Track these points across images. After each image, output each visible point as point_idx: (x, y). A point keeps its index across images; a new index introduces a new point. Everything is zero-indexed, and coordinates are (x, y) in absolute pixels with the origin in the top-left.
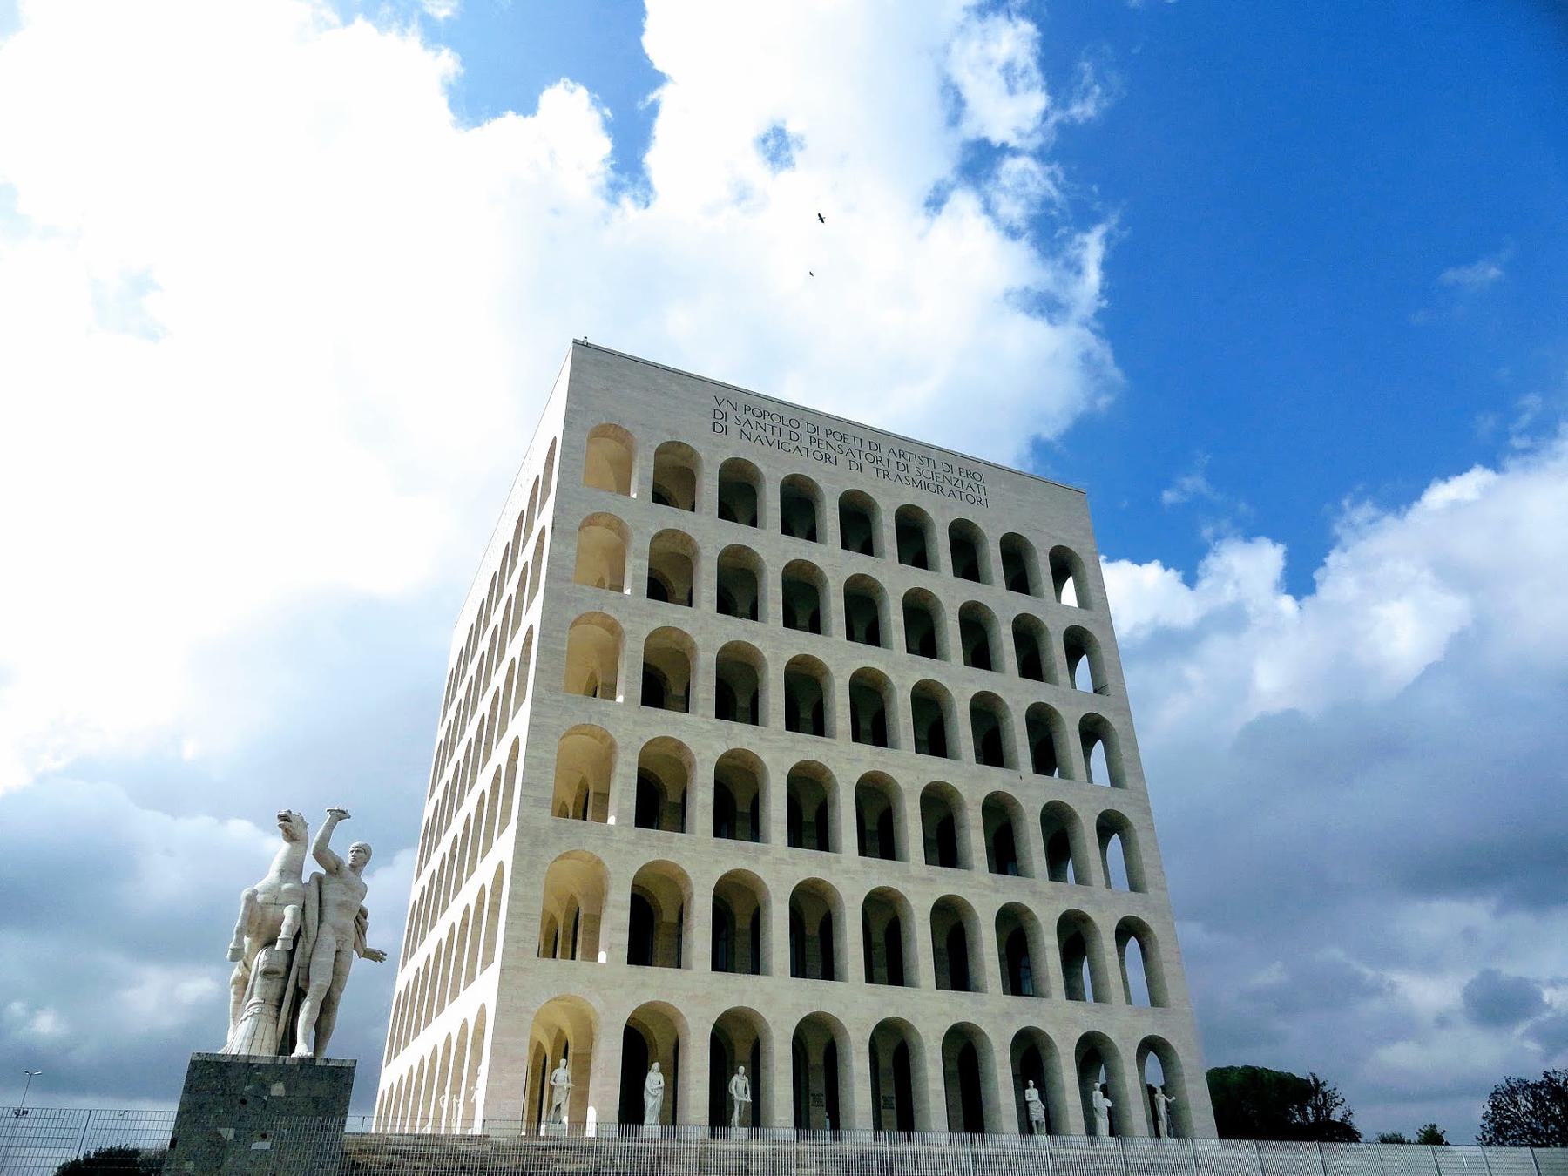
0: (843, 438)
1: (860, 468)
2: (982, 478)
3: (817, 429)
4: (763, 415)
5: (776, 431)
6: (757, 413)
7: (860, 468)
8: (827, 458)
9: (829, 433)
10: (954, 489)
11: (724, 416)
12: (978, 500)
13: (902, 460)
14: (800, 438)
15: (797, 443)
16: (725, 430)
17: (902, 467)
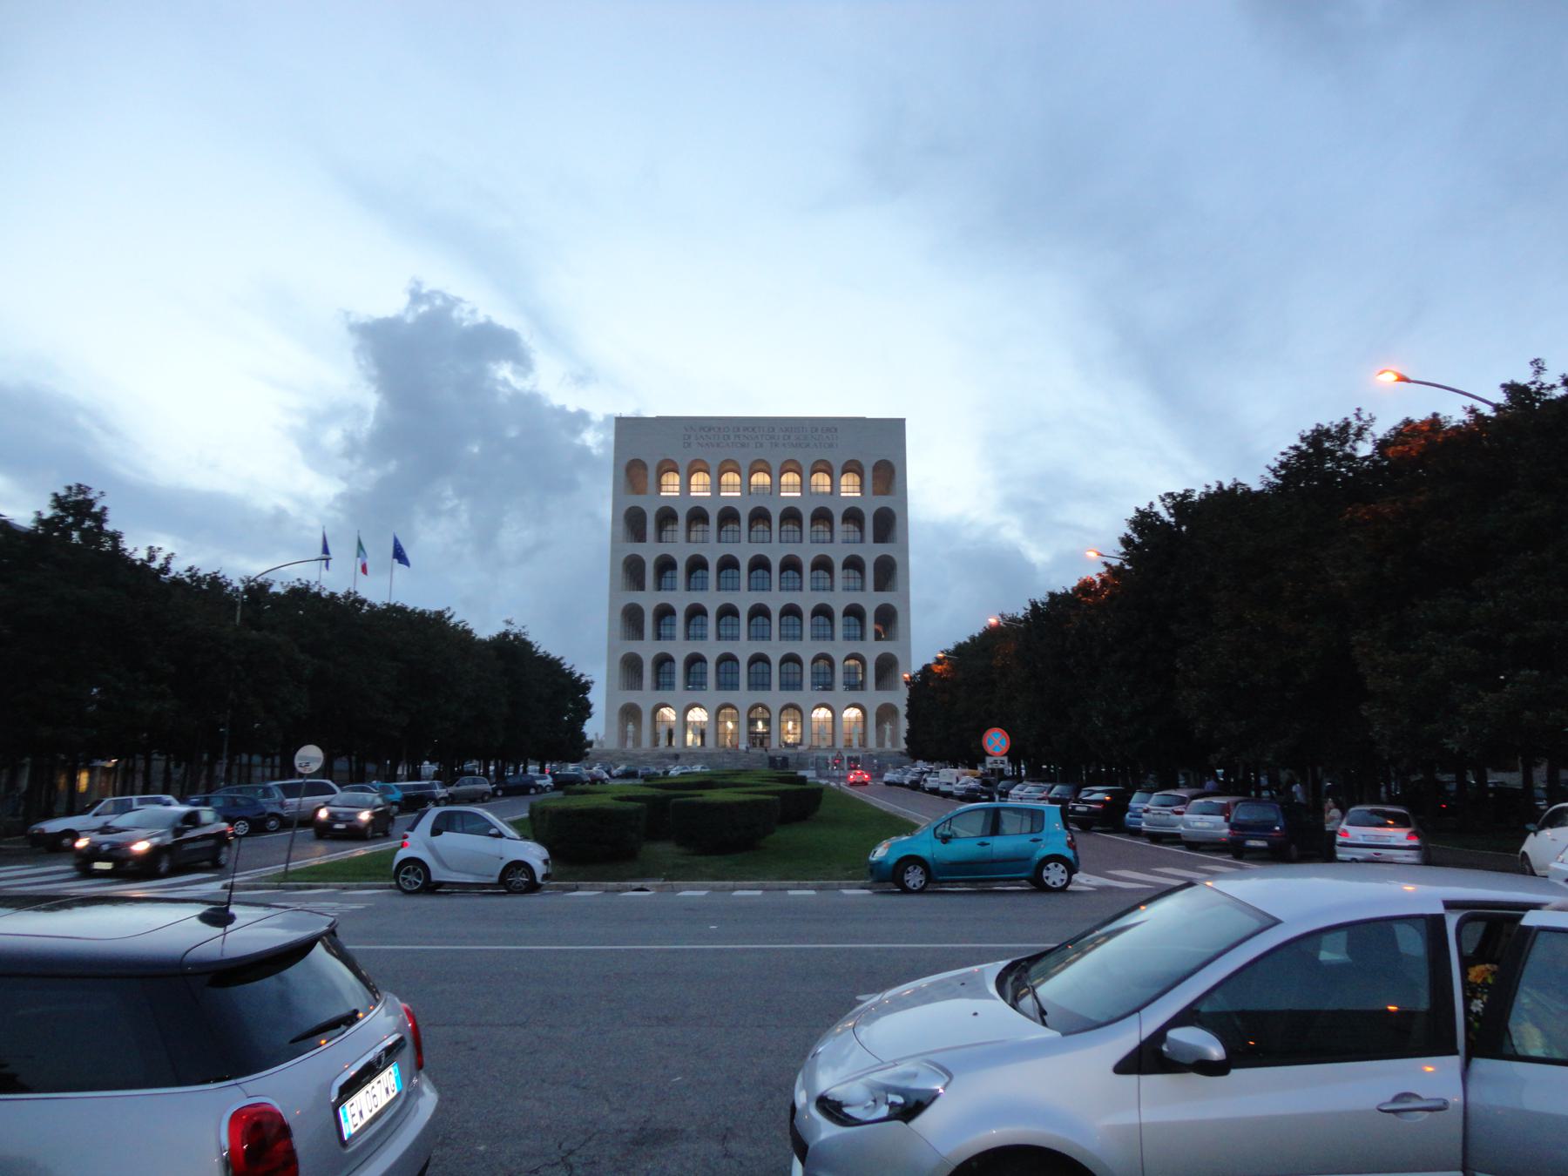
0: (753, 430)
1: (761, 445)
2: (836, 430)
3: (738, 429)
4: (710, 430)
5: (717, 437)
6: (706, 429)
7: (761, 445)
8: (743, 445)
9: (746, 429)
10: (817, 442)
11: (689, 437)
12: (831, 446)
13: (788, 434)
14: (729, 437)
15: (729, 441)
16: (689, 445)
17: (786, 437)
